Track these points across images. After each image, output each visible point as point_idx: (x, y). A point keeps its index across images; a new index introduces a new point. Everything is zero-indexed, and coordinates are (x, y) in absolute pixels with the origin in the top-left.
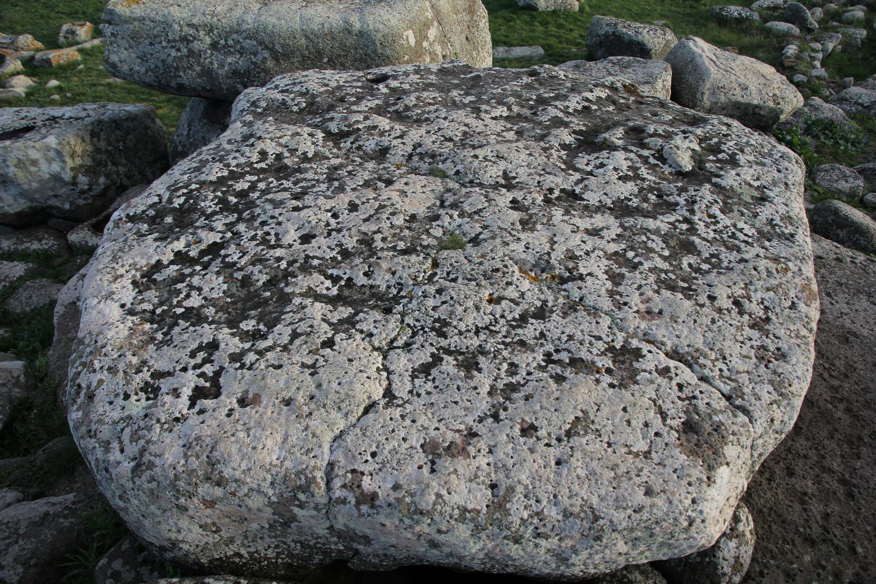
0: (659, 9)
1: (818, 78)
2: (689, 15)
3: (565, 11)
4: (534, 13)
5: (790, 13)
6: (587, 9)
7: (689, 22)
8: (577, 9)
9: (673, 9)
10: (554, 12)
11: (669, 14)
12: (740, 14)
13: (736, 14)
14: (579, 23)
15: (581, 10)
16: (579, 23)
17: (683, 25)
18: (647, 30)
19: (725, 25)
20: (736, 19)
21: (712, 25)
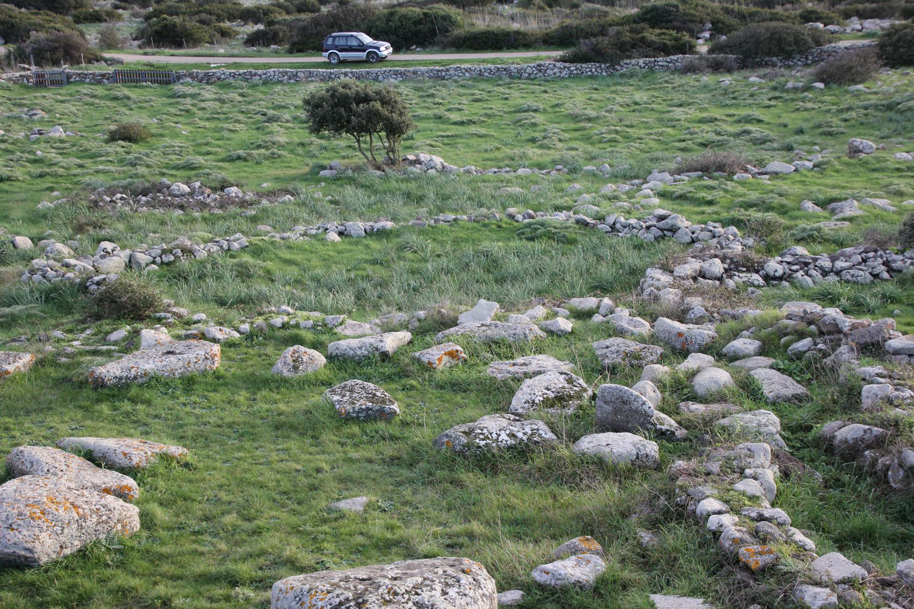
0: (322, 461)
1: (848, 582)
2: (395, 461)
3: (110, 540)
4: (29, 575)
5: (608, 408)
6: (161, 514)
7: (411, 481)
8: (136, 524)
9: (354, 455)
10: (83, 554)
11: (353, 471)
12: (512, 435)
13: (504, 436)
14: (166, 568)
15: (147, 521)
16: (166, 568)
17: (407, 492)
18: (438, 587)
19: (495, 471)
20: (509, 448)
21: (471, 478)
